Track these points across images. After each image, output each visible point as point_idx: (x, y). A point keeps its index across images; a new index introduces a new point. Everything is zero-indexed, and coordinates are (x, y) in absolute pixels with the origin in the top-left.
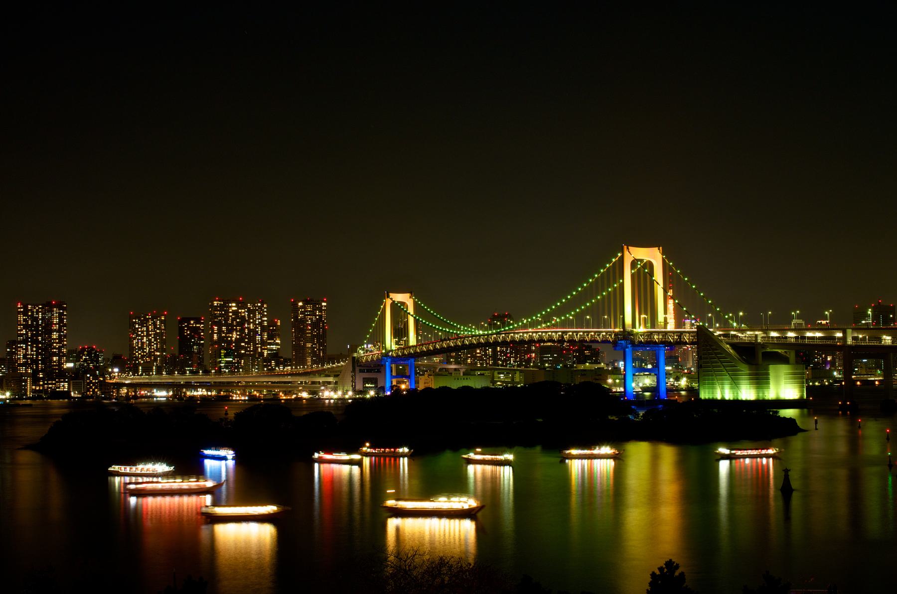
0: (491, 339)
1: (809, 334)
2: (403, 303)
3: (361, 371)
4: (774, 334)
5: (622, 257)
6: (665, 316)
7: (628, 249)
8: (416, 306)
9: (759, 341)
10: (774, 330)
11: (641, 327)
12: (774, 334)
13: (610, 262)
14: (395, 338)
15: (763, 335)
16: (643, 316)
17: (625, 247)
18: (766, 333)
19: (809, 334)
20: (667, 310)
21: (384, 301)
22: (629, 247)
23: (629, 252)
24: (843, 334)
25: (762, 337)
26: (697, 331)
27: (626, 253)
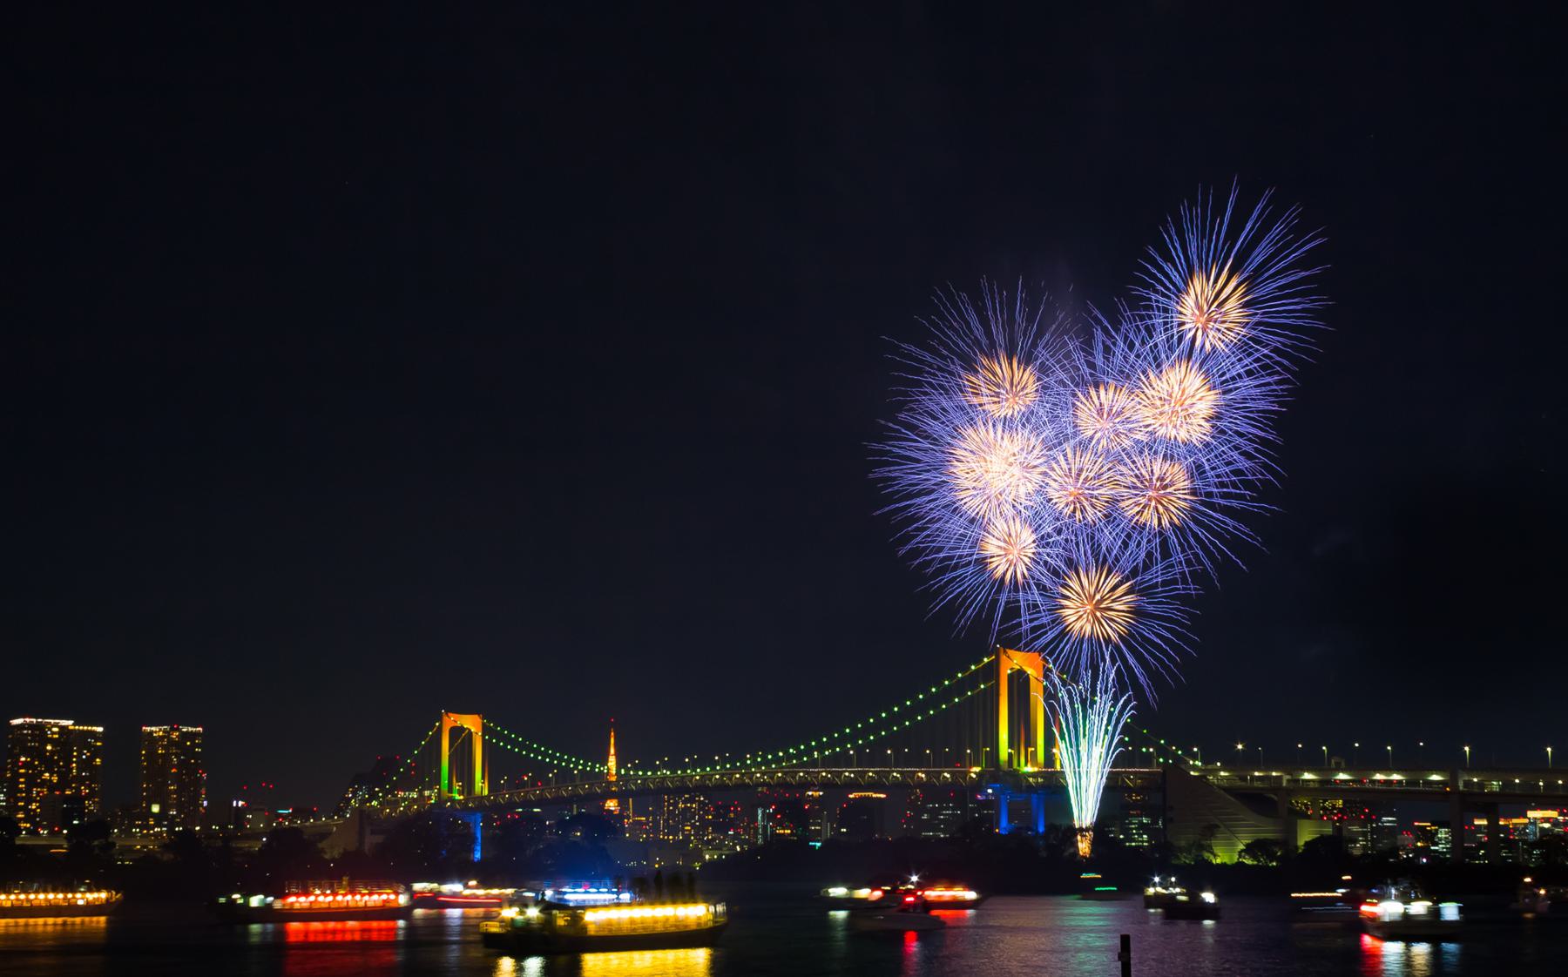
0: (691, 781)
1: (1379, 777)
2: (462, 729)
3: (373, 832)
4: (1307, 776)
5: (998, 660)
6: (1010, 751)
7: (1005, 652)
8: (485, 730)
9: (1284, 784)
10: (1309, 771)
11: (1029, 765)
12: (1307, 776)
13: (965, 669)
14: (457, 781)
15: (1288, 777)
16: (1030, 749)
17: (1002, 649)
18: (1291, 775)
19: (1379, 777)
20: (1030, 739)
21: (437, 724)
22: (1007, 650)
23: (1008, 657)
24: (1451, 777)
25: (1288, 780)
26: (1164, 771)
27: (1003, 657)
